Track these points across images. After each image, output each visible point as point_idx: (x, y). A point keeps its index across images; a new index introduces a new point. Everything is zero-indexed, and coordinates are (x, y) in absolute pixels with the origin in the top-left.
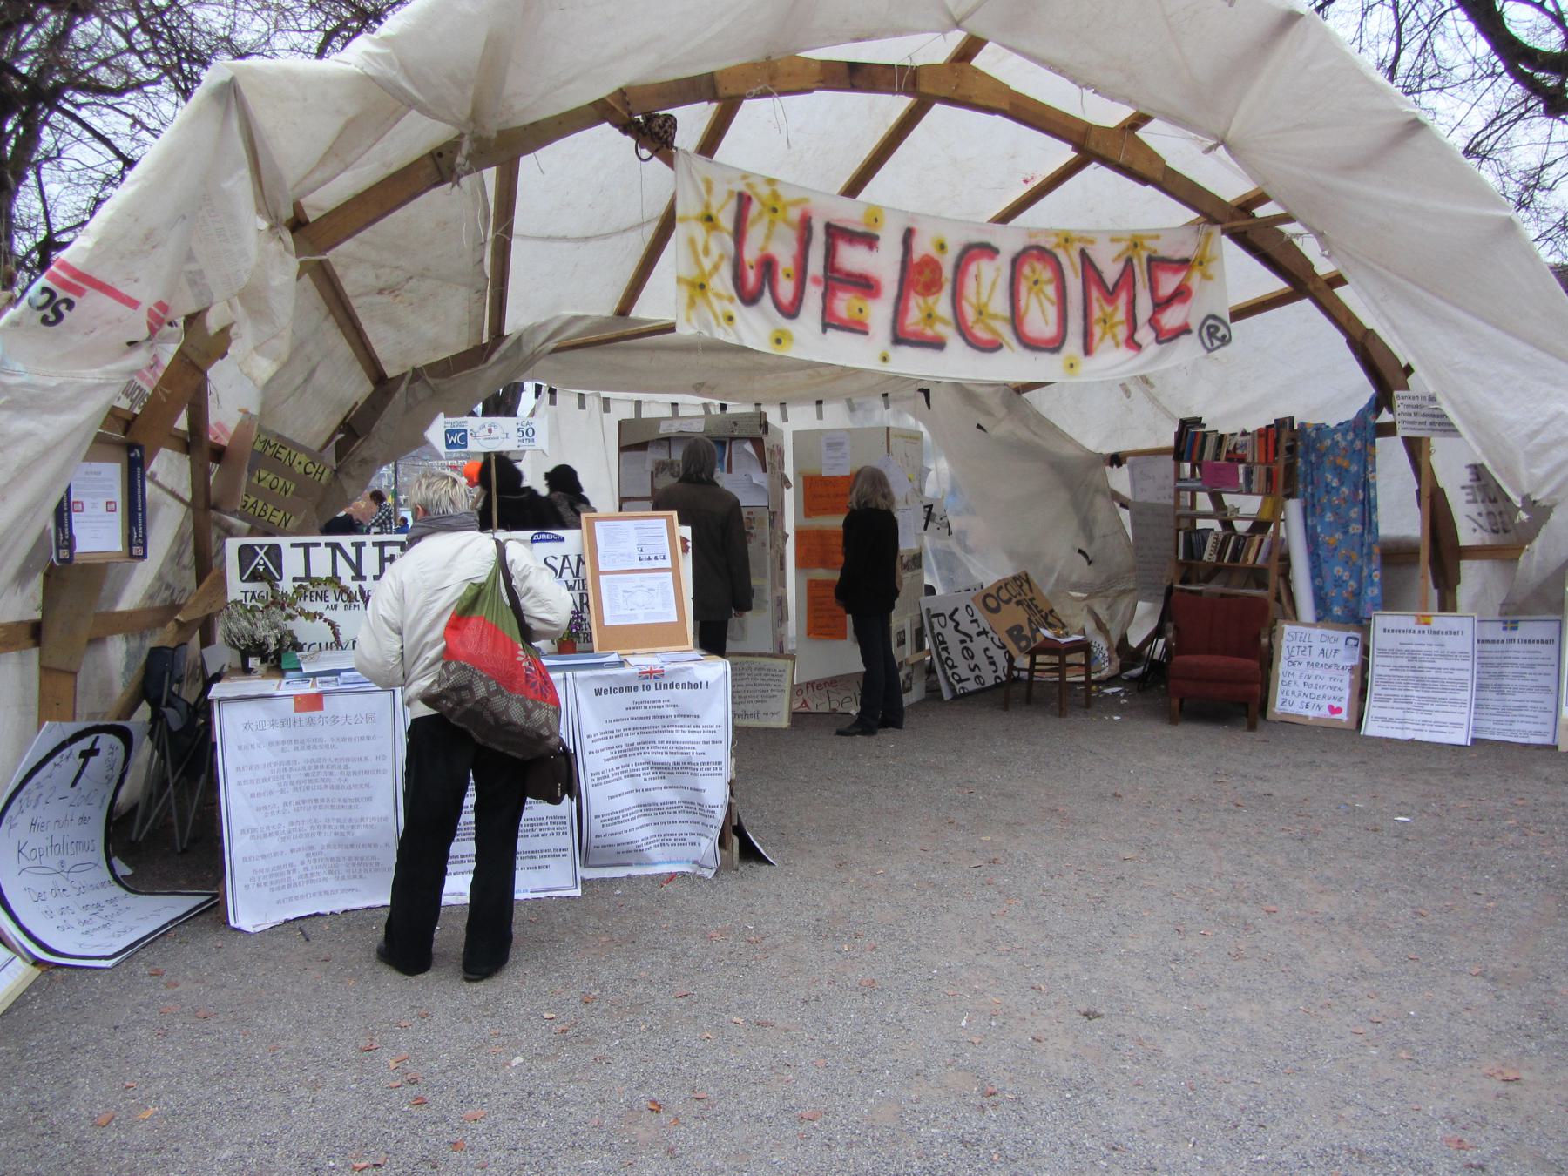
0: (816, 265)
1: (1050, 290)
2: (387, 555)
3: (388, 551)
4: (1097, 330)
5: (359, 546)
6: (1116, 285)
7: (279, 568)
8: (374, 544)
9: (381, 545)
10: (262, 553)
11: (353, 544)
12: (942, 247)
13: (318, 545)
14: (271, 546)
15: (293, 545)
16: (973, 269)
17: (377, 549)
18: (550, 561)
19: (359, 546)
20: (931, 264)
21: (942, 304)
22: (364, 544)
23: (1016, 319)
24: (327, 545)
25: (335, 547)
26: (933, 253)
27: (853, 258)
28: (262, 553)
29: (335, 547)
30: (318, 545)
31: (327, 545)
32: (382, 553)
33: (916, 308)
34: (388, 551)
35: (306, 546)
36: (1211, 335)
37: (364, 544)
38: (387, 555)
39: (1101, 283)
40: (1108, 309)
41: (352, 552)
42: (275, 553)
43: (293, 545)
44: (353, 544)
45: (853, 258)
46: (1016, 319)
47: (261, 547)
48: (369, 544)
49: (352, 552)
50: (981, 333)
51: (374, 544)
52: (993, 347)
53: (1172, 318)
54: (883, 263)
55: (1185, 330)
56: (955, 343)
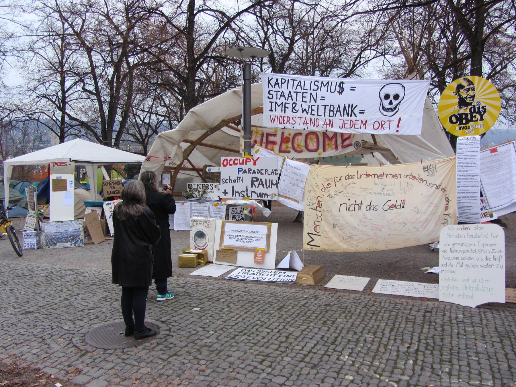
0: (264, 140)
1: (315, 140)
4: (327, 147)
6: (332, 138)
12: (290, 135)
16: (297, 138)
20: (288, 138)
21: (290, 145)
23: (306, 146)
26: (288, 136)
27: (271, 139)
33: (284, 147)
36: (357, 146)
39: (328, 137)
40: (330, 142)
45: (271, 139)
46: (306, 146)
50: (298, 149)
52: (301, 152)
53: (347, 143)
54: (278, 139)
55: (351, 145)
56: (292, 151)
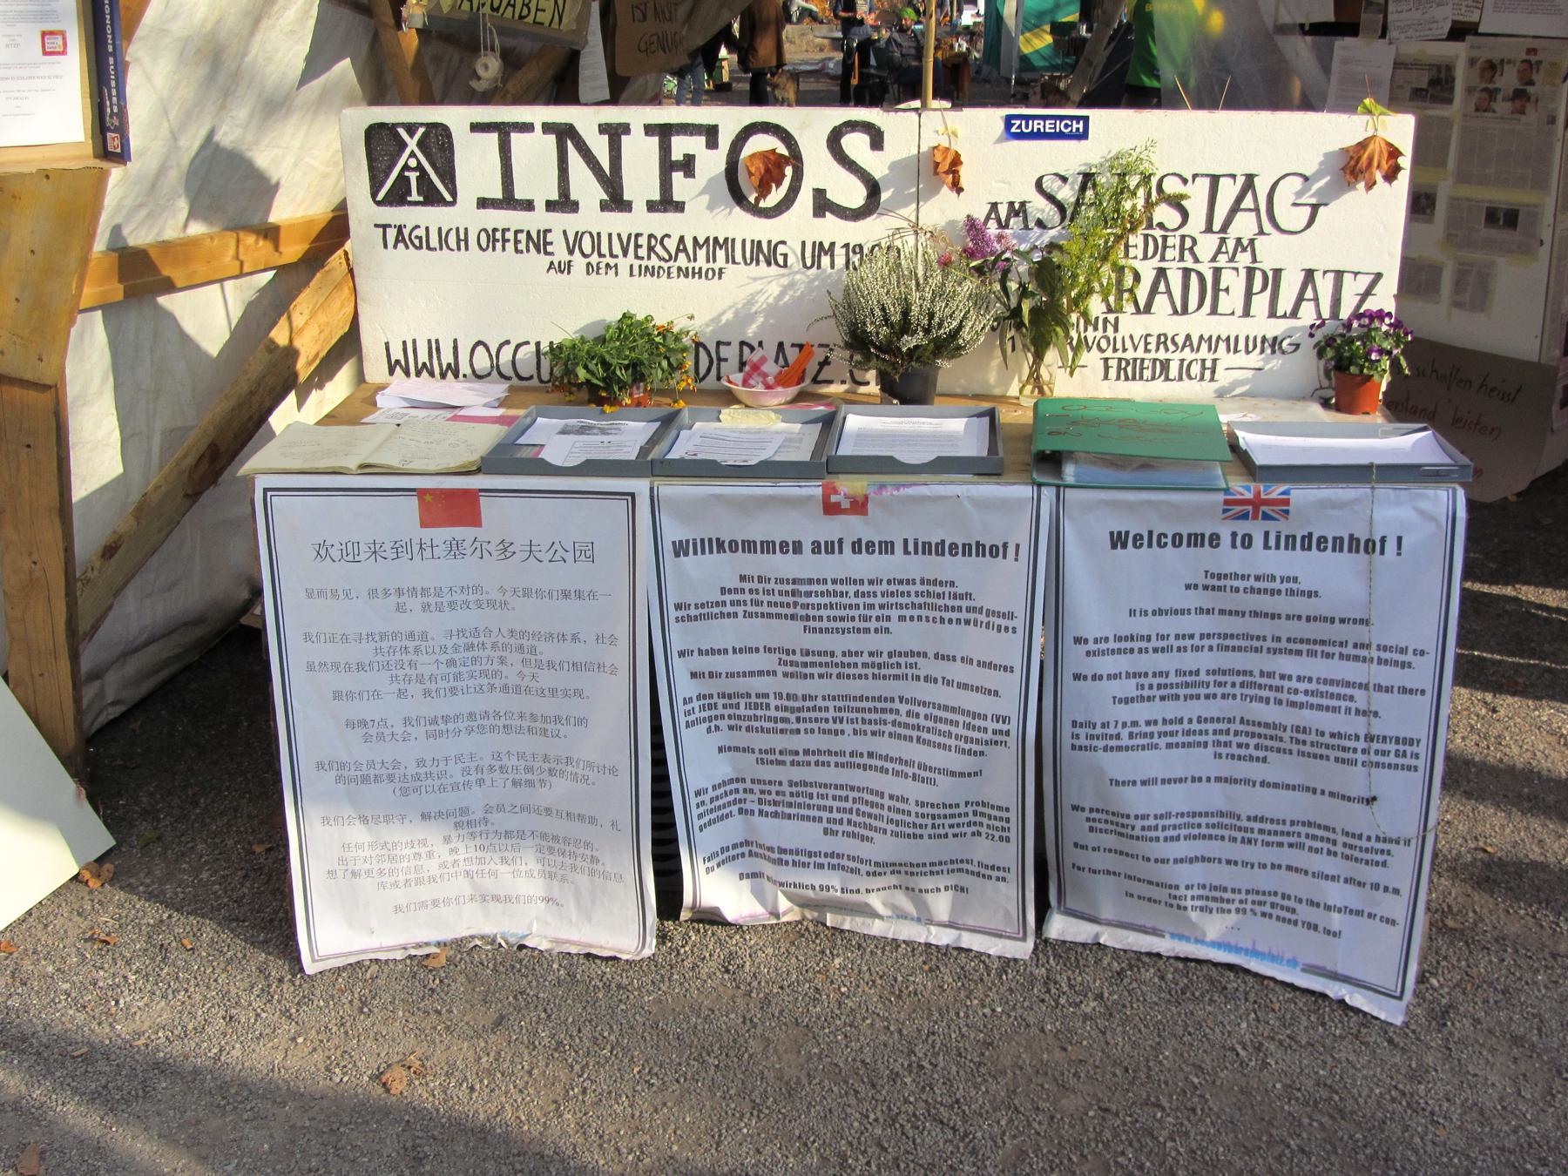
2: (677, 155)
3: (681, 146)
5: (615, 133)
7: (449, 176)
8: (649, 130)
9: (664, 133)
10: (412, 144)
11: (604, 128)
13: (527, 128)
14: (431, 126)
15: (476, 128)
17: (655, 140)
18: (1050, 184)
19: (615, 133)
22: (625, 128)
24: (548, 128)
25: (565, 134)
28: (412, 144)
29: (565, 134)
30: (527, 128)
31: (548, 128)
32: (665, 149)
34: (681, 146)
35: (504, 131)
37: (625, 128)
38: (677, 155)
41: (600, 147)
42: (438, 142)
43: (476, 128)
44: (604, 128)
47: (411, 129)
48: (637, 130)
49: (600, 147)
51: (649, 130)
